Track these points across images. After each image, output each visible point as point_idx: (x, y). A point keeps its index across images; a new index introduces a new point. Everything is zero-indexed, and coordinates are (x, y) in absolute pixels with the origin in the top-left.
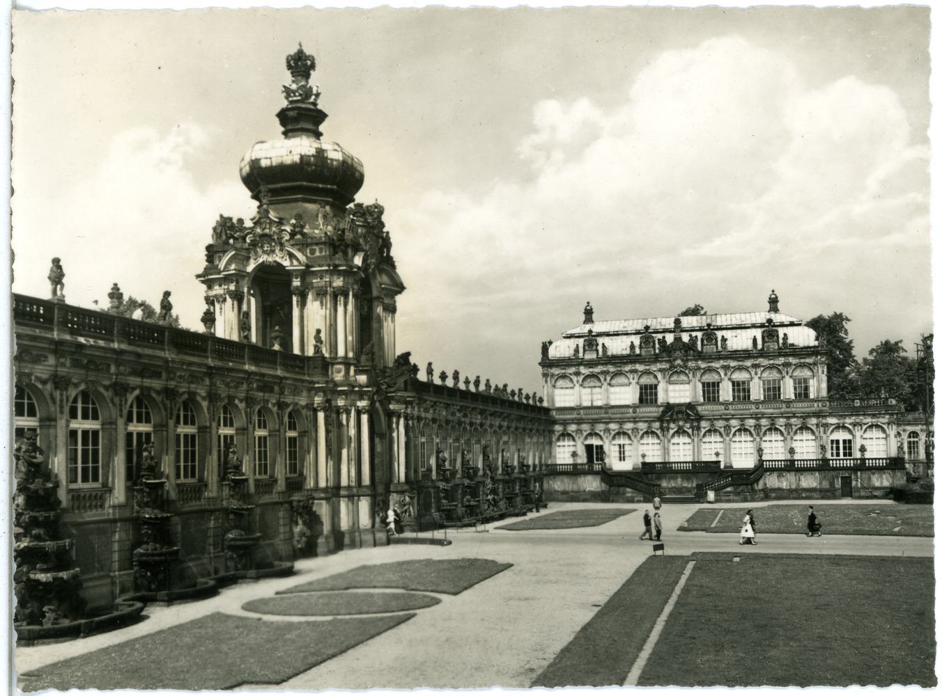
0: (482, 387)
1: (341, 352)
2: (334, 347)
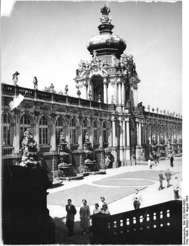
0: (166, 113)
1: (120, 103)
2: (117, 101)
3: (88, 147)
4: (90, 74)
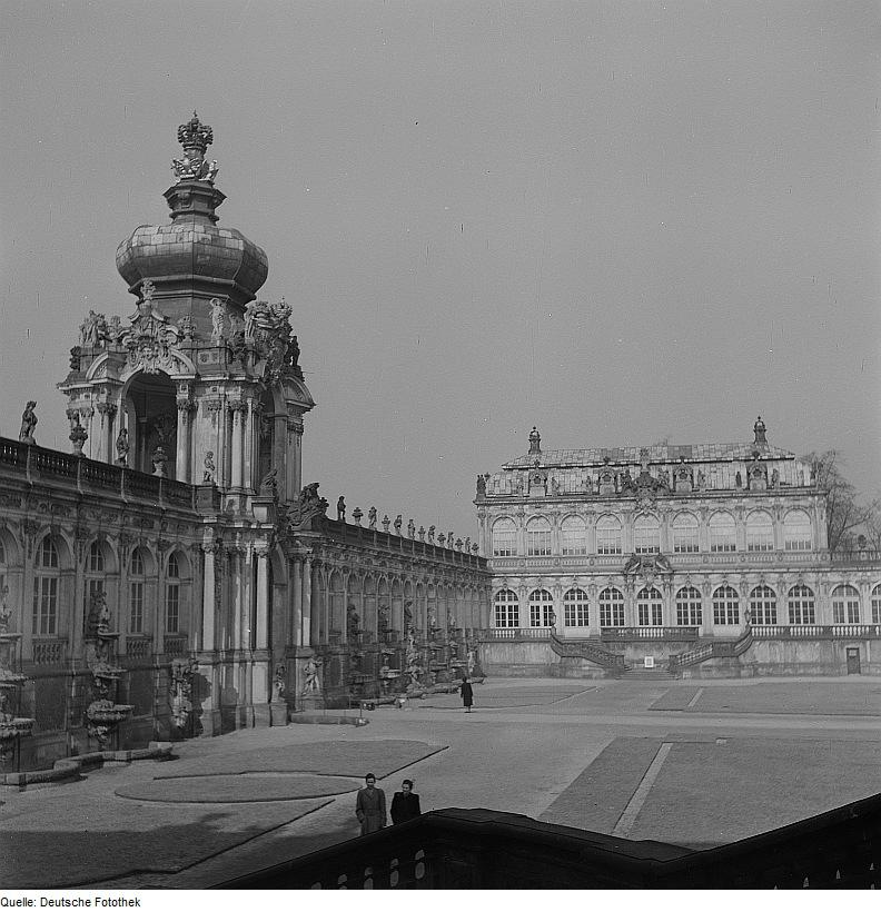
1: (236, 482)
2: (228, 475)
3: (105, 650)
4: (128, 367)
